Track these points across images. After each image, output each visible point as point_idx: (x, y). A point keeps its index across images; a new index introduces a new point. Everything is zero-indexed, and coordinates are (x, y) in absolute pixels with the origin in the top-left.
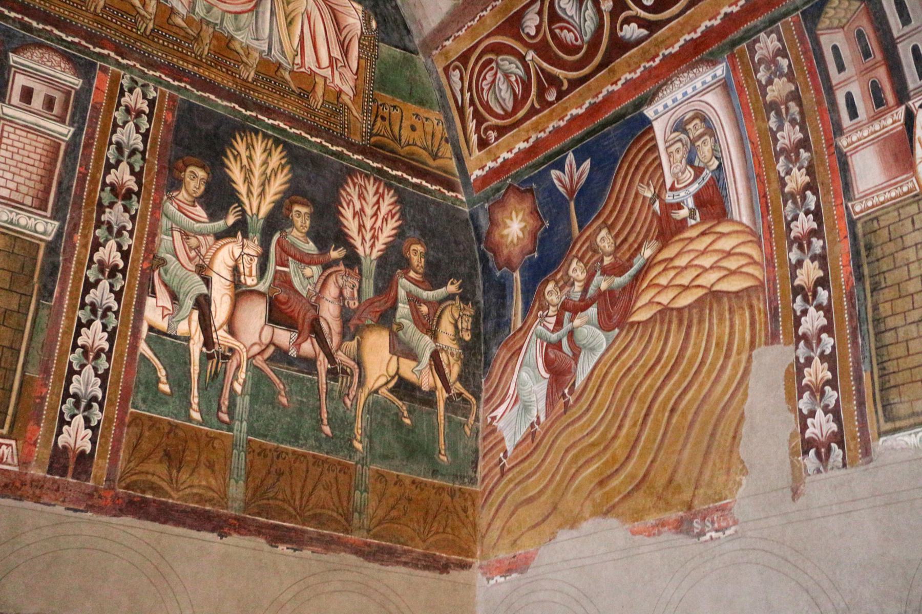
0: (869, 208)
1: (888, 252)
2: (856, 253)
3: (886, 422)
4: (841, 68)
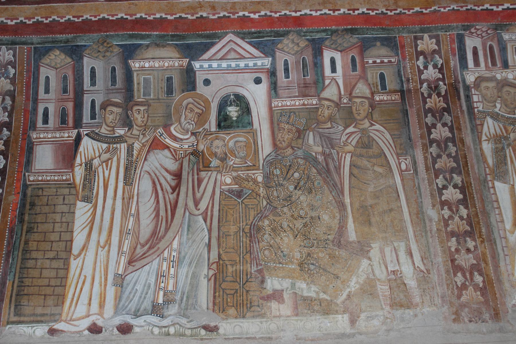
0: (39, 181)
1: (44, 211)
2: (23, 205)
3: (15, 316)
4: (47, 91)
